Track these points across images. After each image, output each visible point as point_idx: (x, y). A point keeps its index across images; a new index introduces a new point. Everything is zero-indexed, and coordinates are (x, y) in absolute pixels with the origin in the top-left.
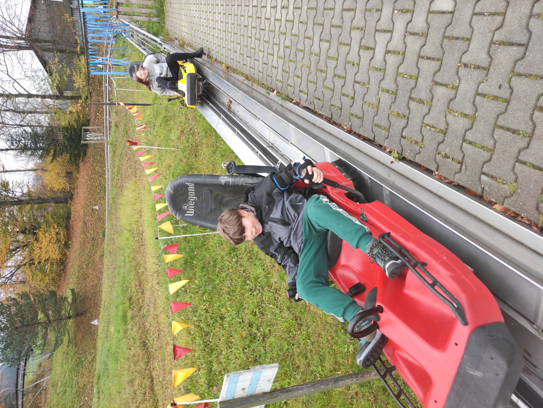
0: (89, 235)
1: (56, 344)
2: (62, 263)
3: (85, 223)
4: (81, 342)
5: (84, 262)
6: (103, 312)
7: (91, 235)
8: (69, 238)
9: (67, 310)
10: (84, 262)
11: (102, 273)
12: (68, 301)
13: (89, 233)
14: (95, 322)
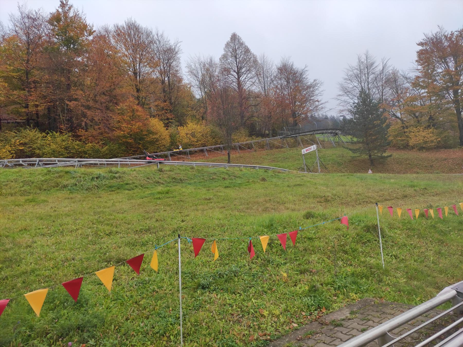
0: (435, 163)
1: (354, 149)
2: (406, 147)
3: (445, 159)
4: (352, 164)
5: (411, 161)
6: (378, 175)
7: (435, 164)
8: (428, 149)
9: (377, 154)
10: (411, 161)
11: (404, 173)
12: (383, 153)
13: (437, 163)
14: (370, 172)
